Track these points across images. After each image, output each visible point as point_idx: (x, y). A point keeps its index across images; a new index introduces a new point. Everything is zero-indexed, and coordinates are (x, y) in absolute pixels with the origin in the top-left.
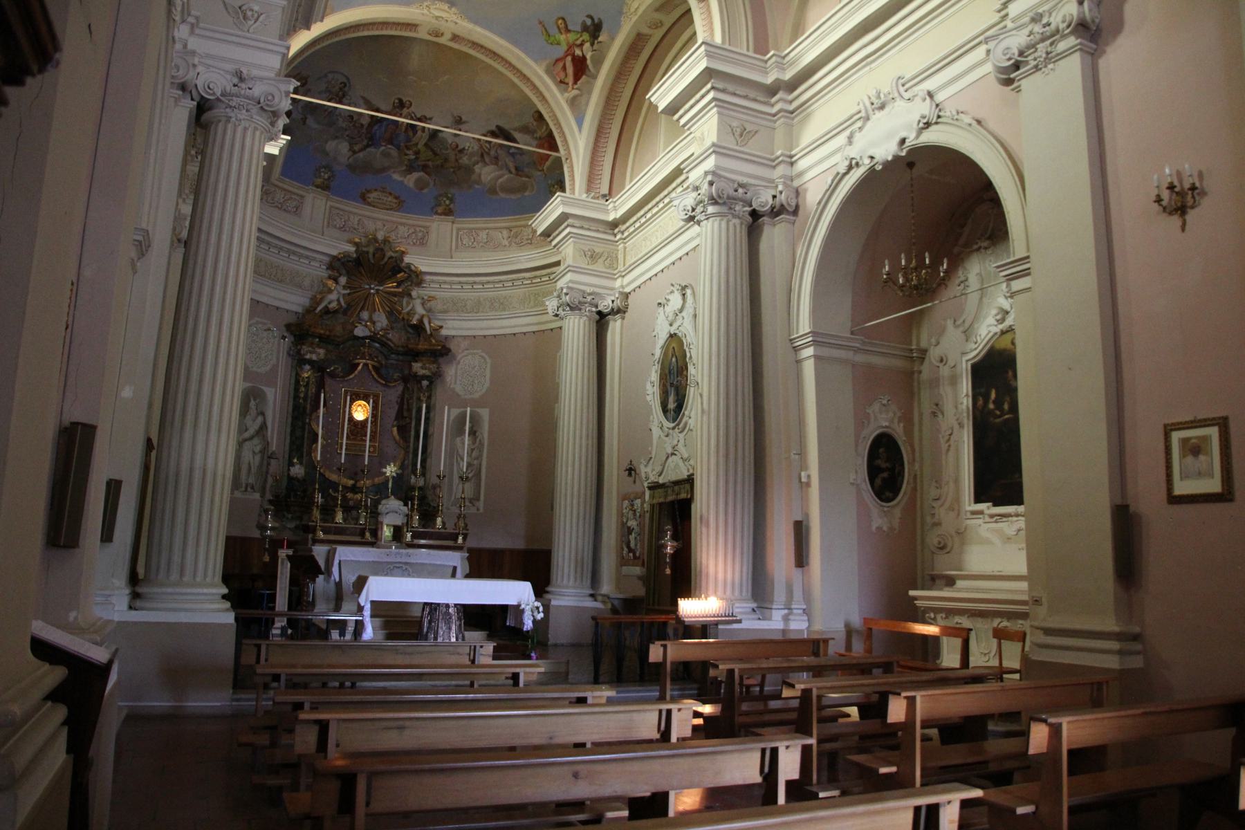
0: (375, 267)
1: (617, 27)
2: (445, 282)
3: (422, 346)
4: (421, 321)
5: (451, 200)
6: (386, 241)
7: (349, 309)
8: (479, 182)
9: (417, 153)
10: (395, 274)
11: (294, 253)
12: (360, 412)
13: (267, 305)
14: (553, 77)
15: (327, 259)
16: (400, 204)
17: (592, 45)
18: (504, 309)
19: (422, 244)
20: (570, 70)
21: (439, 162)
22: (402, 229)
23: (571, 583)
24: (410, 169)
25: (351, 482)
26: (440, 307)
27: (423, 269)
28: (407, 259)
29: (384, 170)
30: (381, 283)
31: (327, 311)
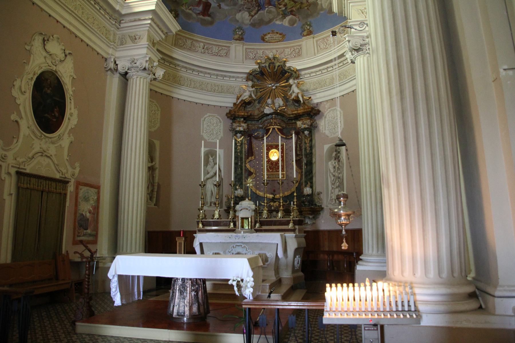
0: (273, 74)
2: (312, 73)
3: (301, 110)
4: (298, 97)
5: (310, 26)
6: (274, 58)
7: (261, 100)
8: (322, 9)
9: (285, 5)
10: (283, 76)
11: (225, 76)
12: (275, 155)
13: (215, 106)
15: (245, 76)
16: (284, 37)
18: (346, 78)
19: (299, 55)
21: (298, 6)
22: (287, 50)
23: (375, 252)
24: (284, 16)
25: (271, 196)
26: (312, 87)
27: (298, 68)
28: (288, 65)
29: (270, 21)
30: (278, 81)
31: (245, 104)
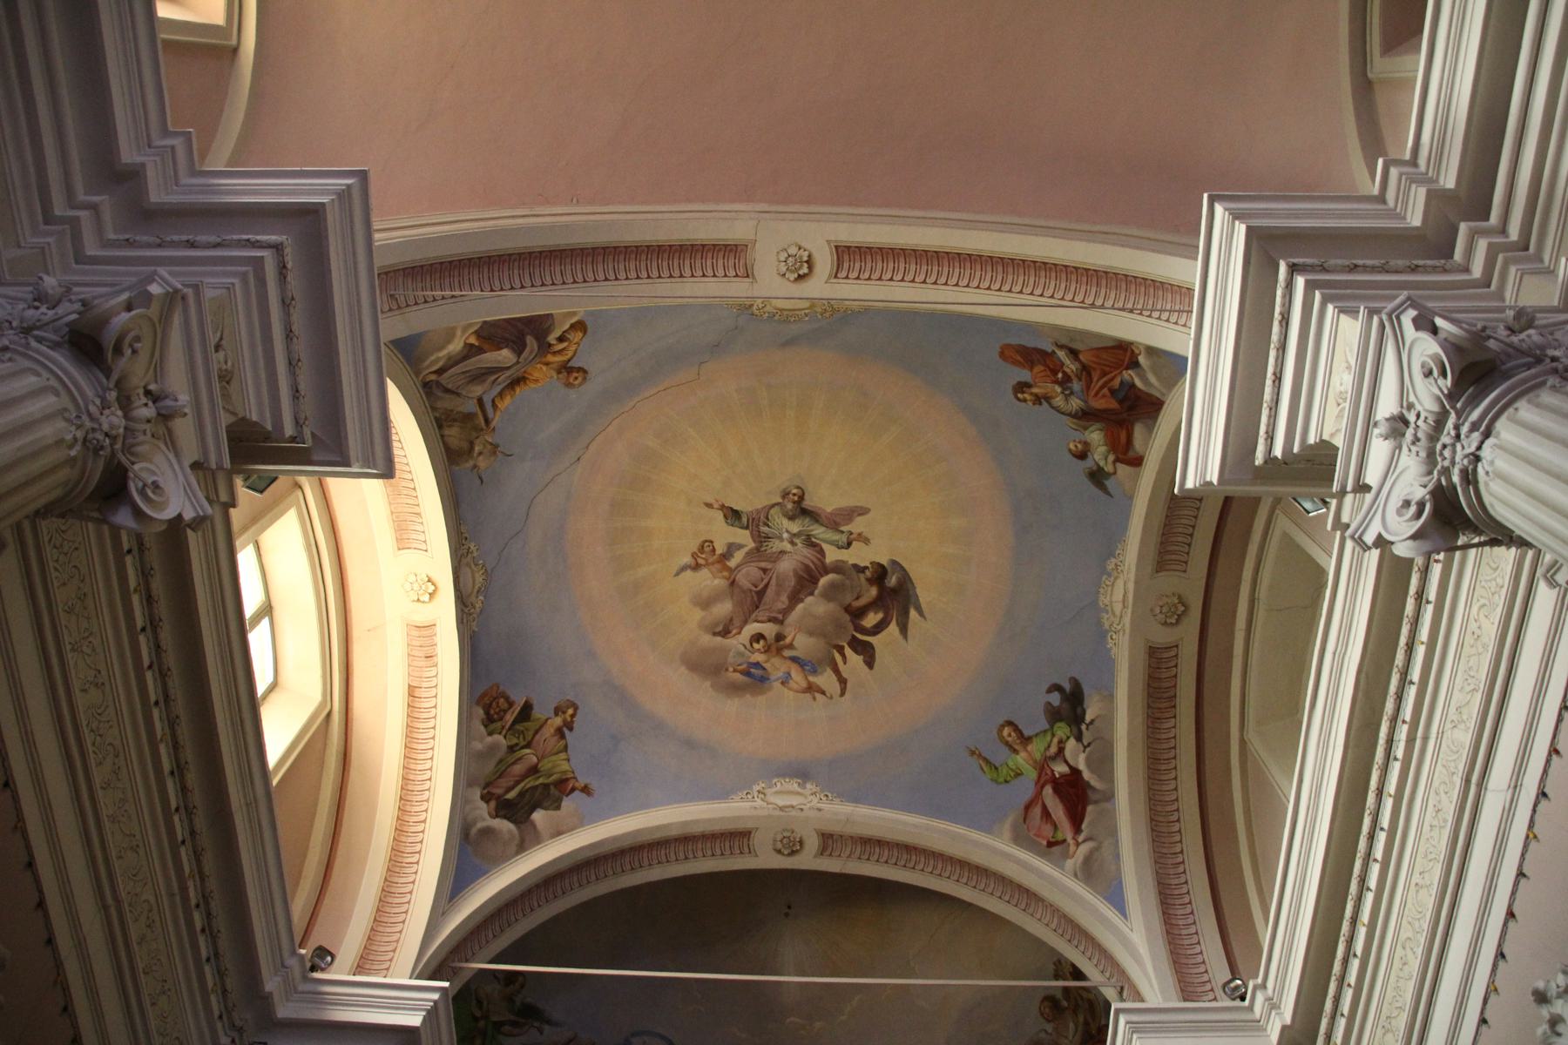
1: (1109, 664)
14: (1030, 846)
17: (1079, 738)
20: (1058, 811)
